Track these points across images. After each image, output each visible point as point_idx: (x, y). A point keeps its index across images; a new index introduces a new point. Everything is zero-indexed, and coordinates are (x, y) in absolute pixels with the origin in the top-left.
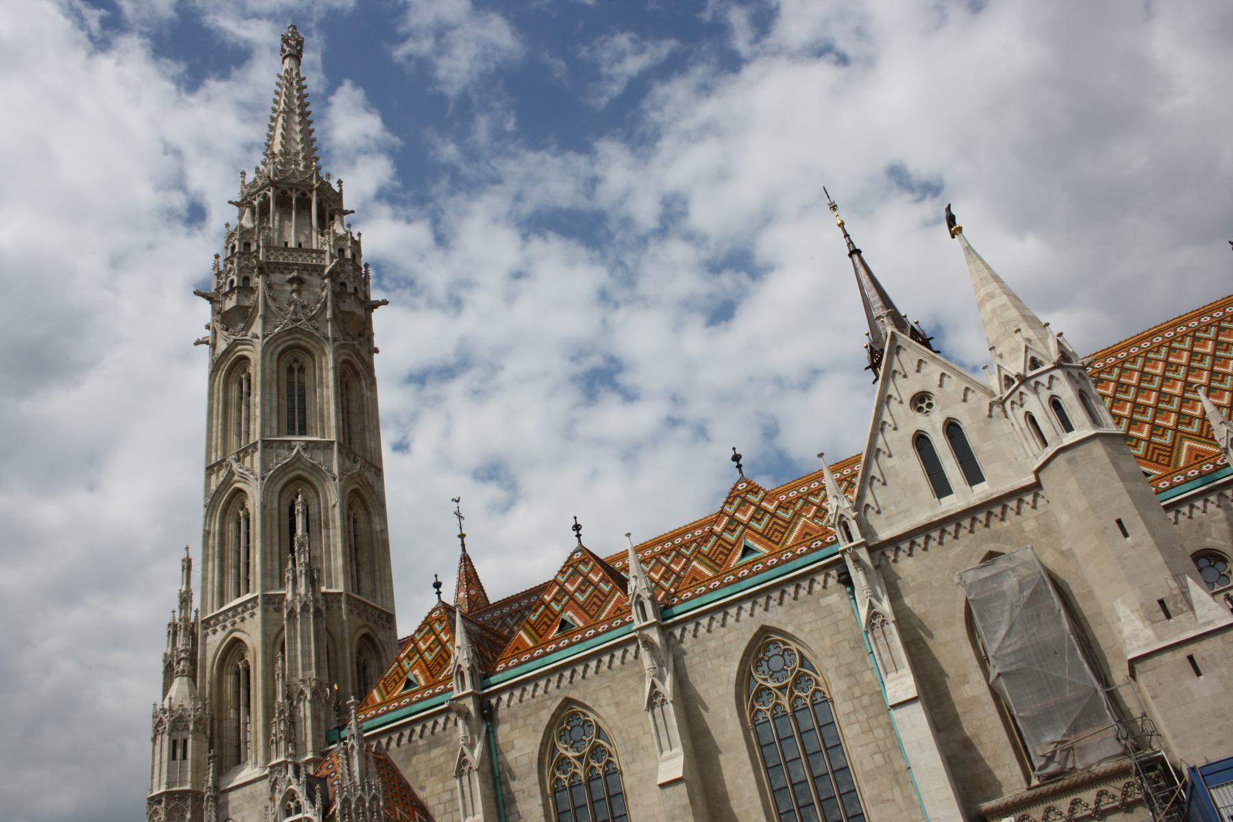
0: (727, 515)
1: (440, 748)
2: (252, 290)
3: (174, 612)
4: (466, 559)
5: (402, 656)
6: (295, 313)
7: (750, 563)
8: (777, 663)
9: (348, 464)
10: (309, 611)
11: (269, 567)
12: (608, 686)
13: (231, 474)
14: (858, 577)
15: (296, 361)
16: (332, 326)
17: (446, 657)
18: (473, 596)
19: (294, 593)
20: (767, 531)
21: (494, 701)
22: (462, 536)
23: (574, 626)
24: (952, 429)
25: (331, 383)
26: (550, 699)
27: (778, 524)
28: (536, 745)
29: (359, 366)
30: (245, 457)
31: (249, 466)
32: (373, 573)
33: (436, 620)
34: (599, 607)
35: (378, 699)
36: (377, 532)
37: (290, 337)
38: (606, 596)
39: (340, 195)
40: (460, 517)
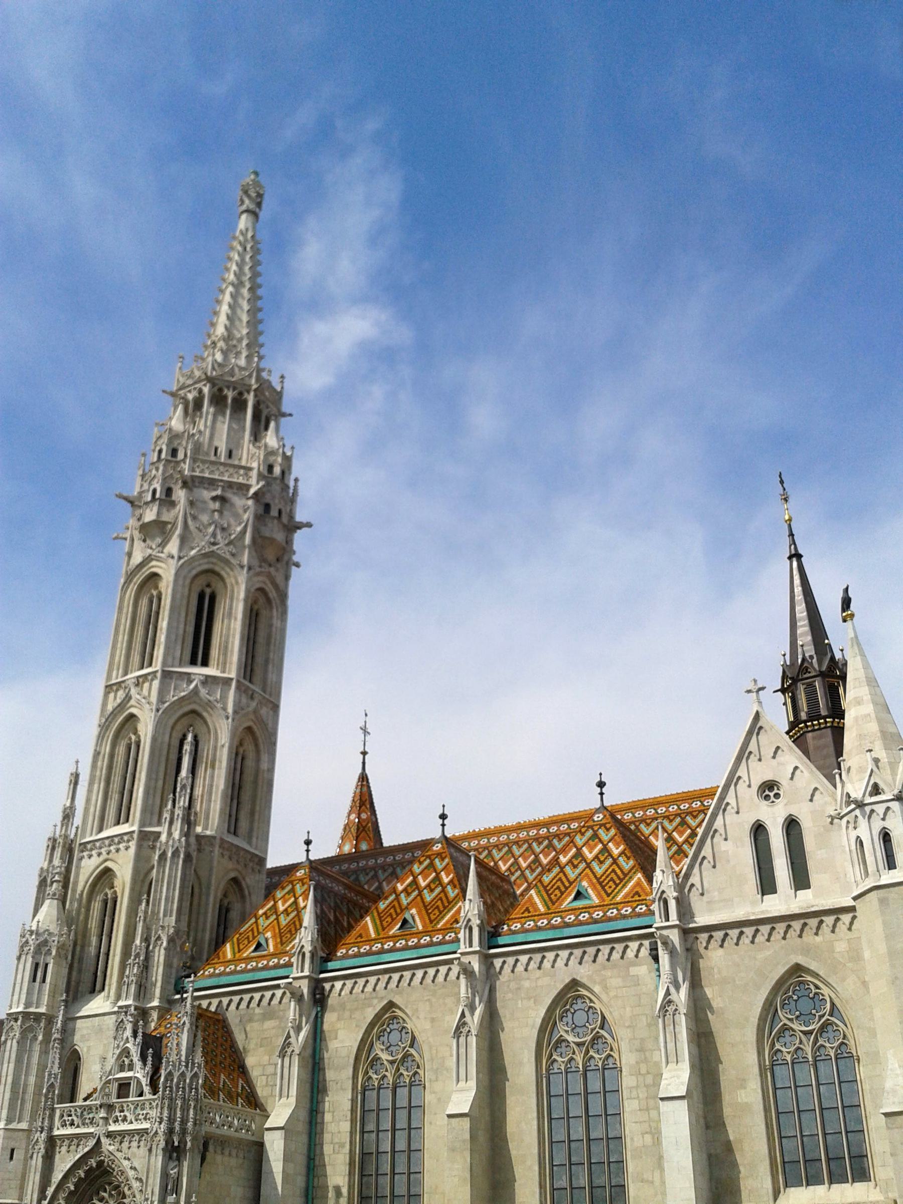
0: (576, 847)
1: (273, 1021)
2: (173, 504)
3: (55, 826)
4: (363, 778)
5: (261, 912)
6: (214, 535)
7: (579, 909)
8: (580, 1017)
9: (244, 700)
10: (179, 856)
11: (150, 802)
12: (429, 1000)
13: (128, 697)
14: (664, 957)
15: (208, 586)
16: (250, 553)
17: (298, 927)
18: (364, 820)
19: (170, 834)
20: (603, 878)
21: (327, 986)
22: (364, 753)
23: (414, 927)
24: (792, 825)
25: (240, 616)
26: (376, 998)
27: (616, 873)
28: (356, 1040)
29: (273, 594)
30: (143, 682)
31: (147, 694)
32: (252, 813)
33: (300, 880)
34: (441, 912)
35: (229, 956)
36: (264, 771)
37: (206, 560)
38: (449, 903)
39: (280, 395)
40: (365, 731)
